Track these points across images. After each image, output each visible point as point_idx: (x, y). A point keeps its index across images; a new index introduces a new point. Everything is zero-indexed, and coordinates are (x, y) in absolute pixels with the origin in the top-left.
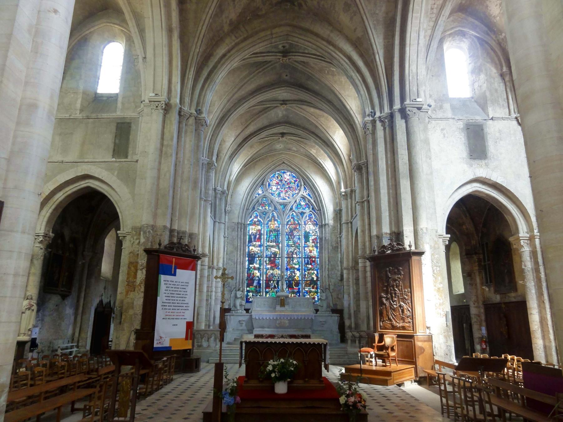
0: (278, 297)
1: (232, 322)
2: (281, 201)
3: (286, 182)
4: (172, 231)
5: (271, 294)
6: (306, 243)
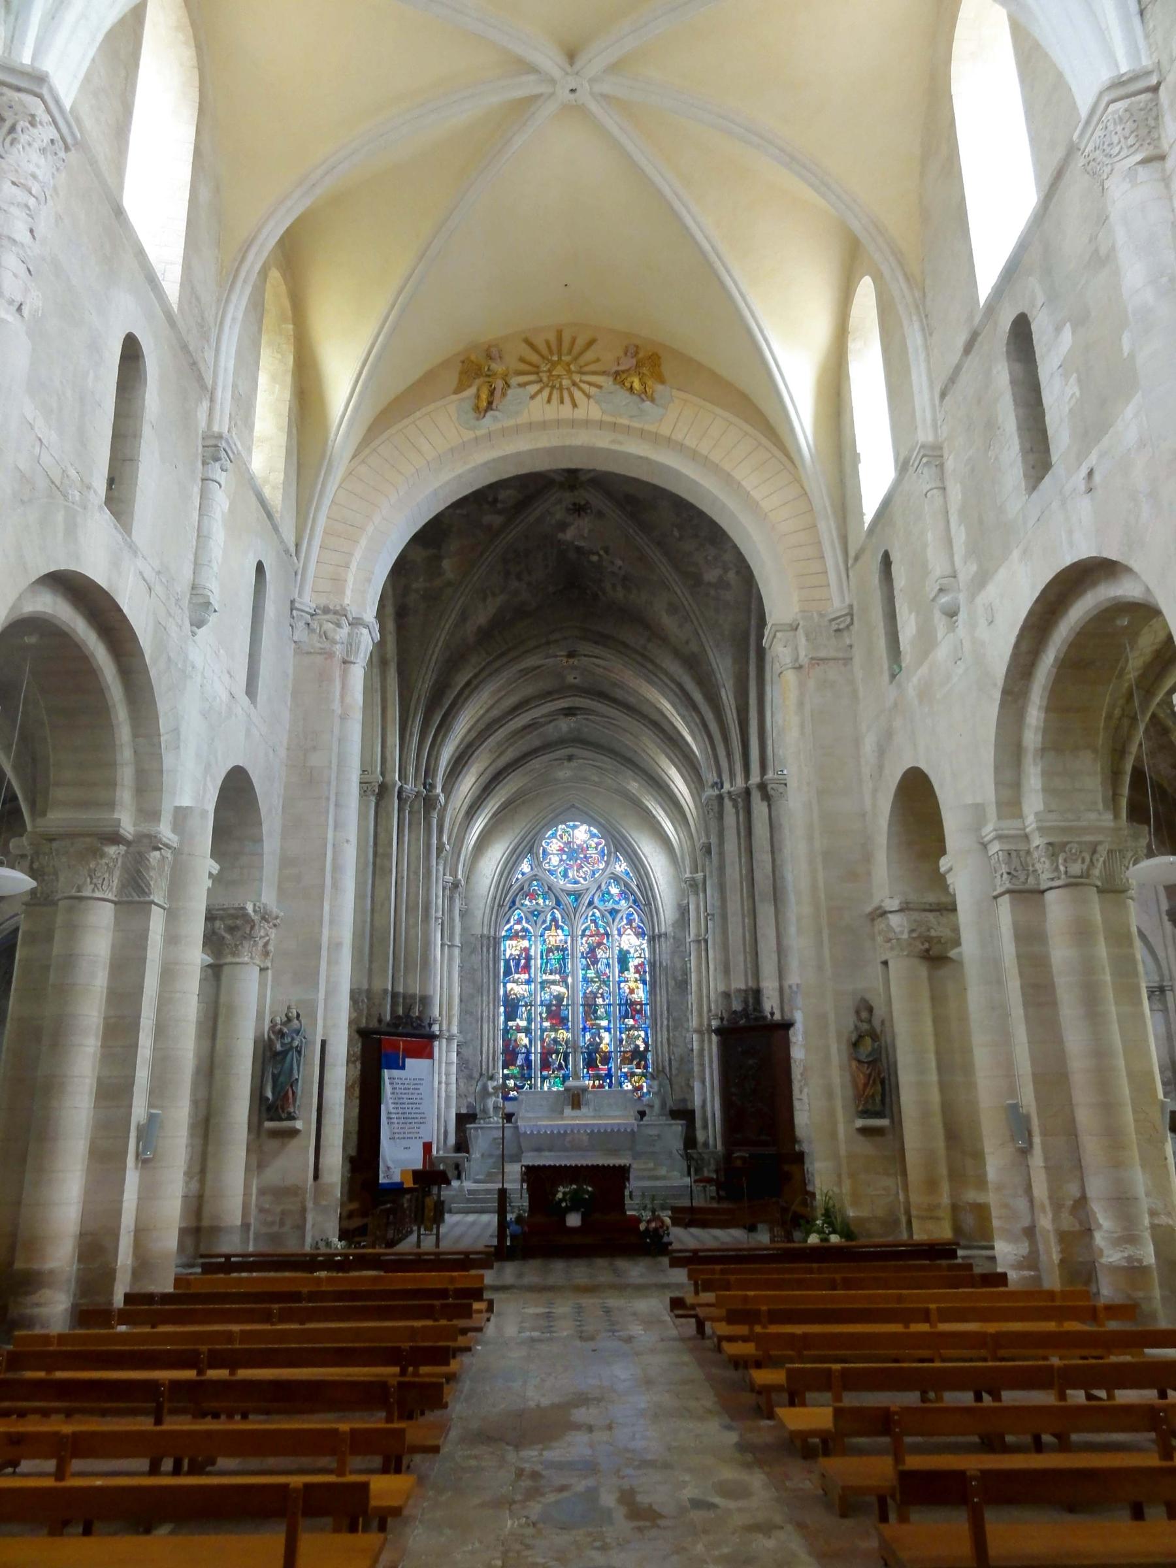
0: (567, 1090)
1: (482, 1141)
2: (570, 886)
3: (578, 845)
4: (395, 995)
5: (552, 1081)
6: (623, 973)
